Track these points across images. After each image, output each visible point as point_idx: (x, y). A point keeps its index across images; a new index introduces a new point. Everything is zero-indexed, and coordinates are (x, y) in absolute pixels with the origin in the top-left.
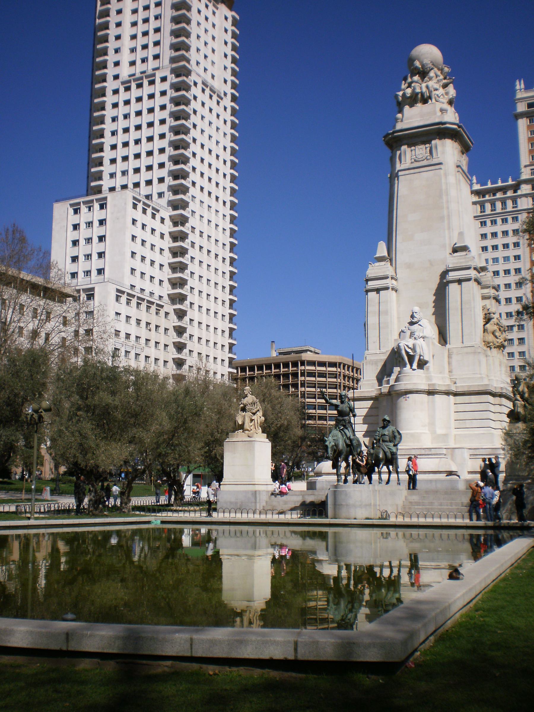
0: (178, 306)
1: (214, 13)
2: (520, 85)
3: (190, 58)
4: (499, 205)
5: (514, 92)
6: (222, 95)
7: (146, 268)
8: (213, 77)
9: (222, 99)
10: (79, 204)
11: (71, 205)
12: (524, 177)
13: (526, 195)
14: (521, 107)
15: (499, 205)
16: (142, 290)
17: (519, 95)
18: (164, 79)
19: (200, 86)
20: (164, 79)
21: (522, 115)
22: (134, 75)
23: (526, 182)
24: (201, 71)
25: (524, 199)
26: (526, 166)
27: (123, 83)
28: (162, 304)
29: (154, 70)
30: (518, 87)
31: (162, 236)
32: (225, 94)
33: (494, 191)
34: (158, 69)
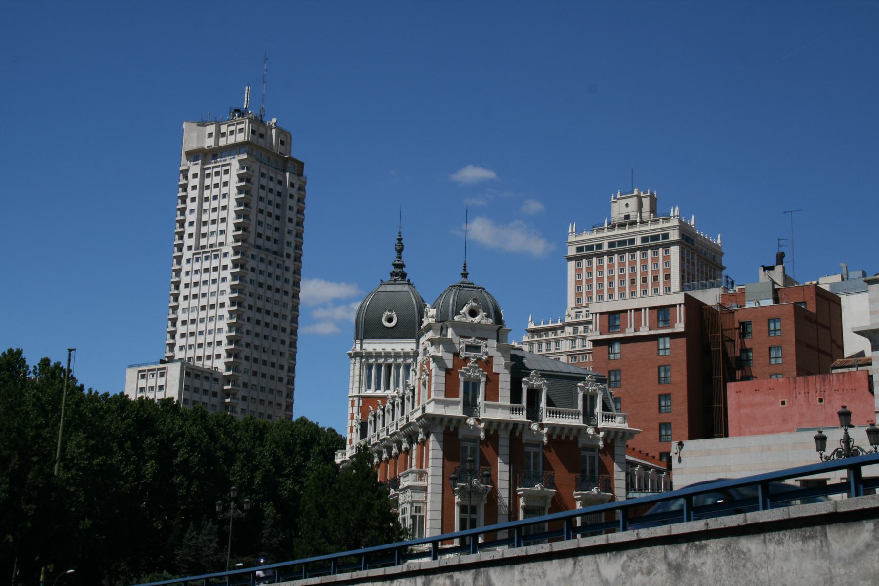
2: (572, 229)
4: (544, 345)
5: (567, 234)
10: (145, 371)
11: (139, 371)
12: (568, 320)
13: (566, 338)
14: (572, 251)
15: (544, 345)
17: (571, 238)
21: (570, 259)
23: (569, 325)
25: (564, 342)
26: (572, 308)
27: (194, 254)
30: (570, 231)
33: (546, 330)
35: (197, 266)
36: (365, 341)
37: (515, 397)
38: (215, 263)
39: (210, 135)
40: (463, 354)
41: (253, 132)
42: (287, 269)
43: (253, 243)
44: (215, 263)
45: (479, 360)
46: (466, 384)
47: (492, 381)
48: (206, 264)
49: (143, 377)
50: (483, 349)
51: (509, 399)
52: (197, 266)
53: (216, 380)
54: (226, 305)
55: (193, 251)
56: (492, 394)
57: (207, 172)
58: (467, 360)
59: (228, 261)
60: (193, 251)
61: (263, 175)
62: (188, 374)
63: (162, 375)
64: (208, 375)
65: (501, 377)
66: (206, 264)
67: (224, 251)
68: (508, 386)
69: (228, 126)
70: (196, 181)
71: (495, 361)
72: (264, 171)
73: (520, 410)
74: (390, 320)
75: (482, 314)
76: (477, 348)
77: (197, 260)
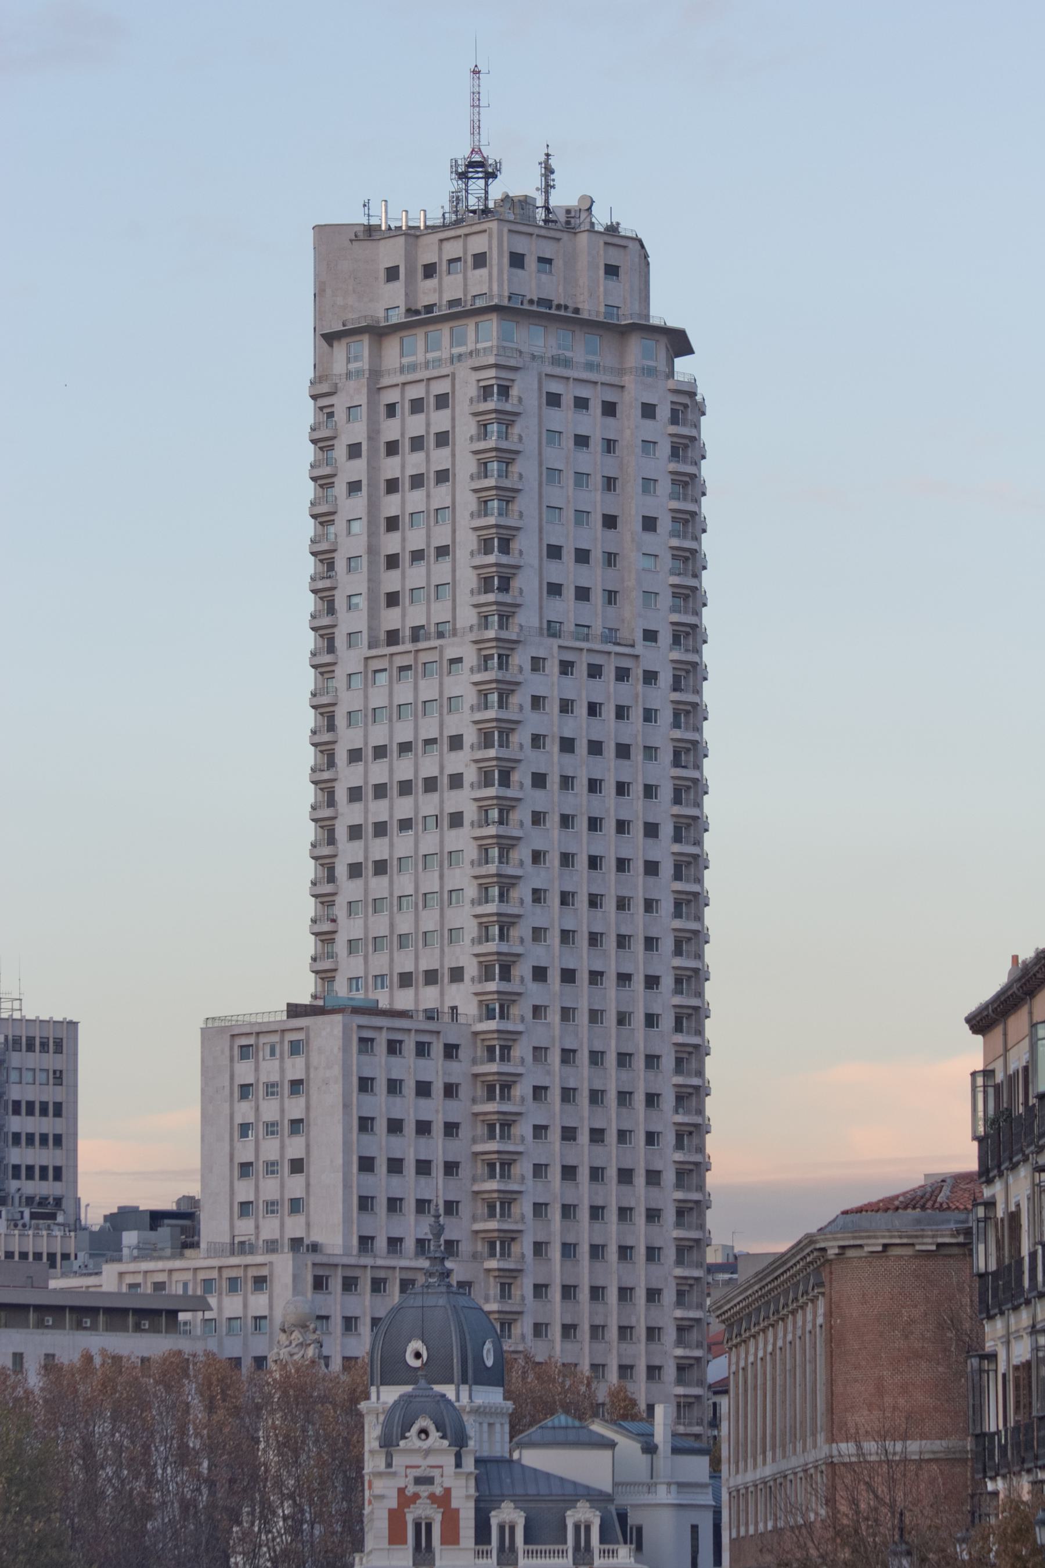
36: (382, 1388)
37: (482, 1534)
39: (392, 274)
40: (411, 1489)
41: (517, 260)
42: (650, 677)
43: (535, 622)
45: (432, 1497)
46: (418, 1526)
47: (451, 1519)
49: (245, 1052)
50: (437, 1480)
51: (473, 1541)
53: (451, 1051)
54: (467, 820)
56: (451, 1537)
58: (416, 1496)
61: (554, 400)
62: (366, 1044)
63: (296, 1048)
65: (462, 1514)
67: (451, 653)
68: (472, 1523)
71: (454, 1493)
72: (555, 387)
73: (488, 1554)
74: (418, 1355)
75: (434, 1434)
76: (429, 1481)
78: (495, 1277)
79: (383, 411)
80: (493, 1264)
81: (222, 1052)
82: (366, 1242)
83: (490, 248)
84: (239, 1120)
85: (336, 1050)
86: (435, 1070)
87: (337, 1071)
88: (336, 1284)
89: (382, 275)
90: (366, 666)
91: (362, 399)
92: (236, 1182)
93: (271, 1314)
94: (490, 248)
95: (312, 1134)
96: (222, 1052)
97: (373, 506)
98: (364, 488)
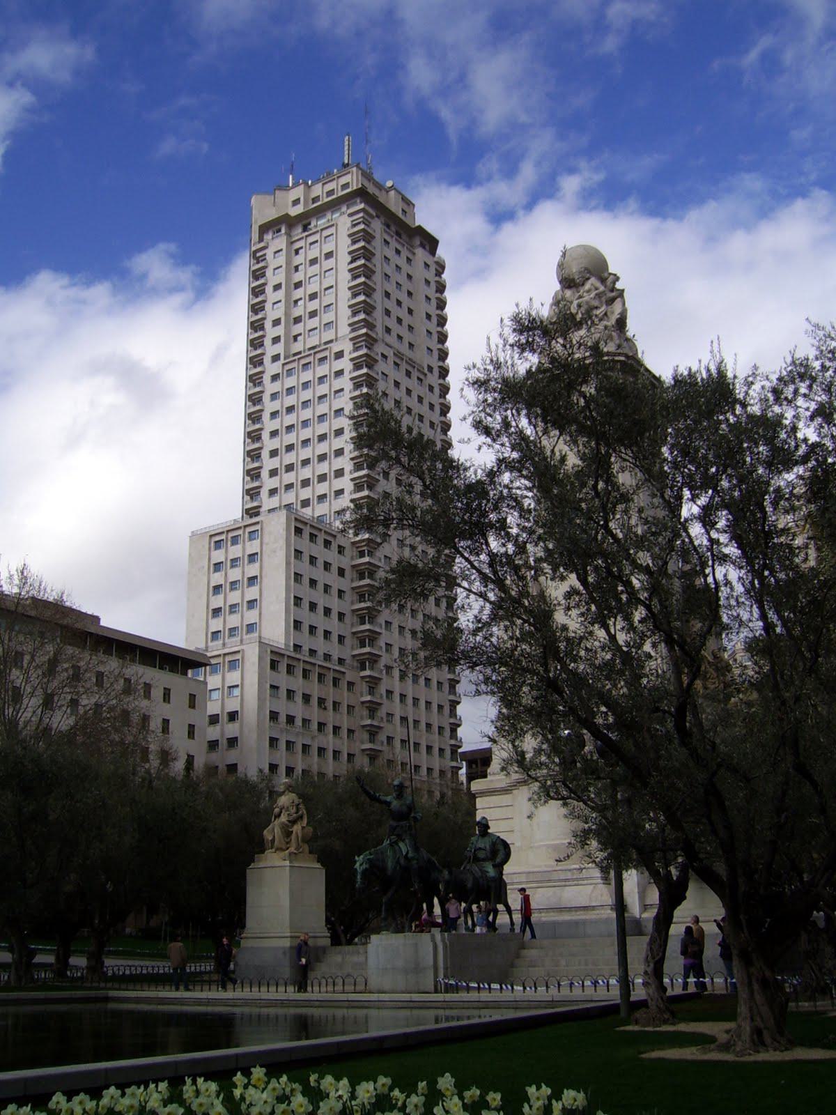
0: (367, 673)
1: (409, 260)
3: (374, 323)
6: (426, 370)
7: (318, 619)
8: (411, 345)
9: (426, 375)
16: (312, 652)
18: (339, 355)
19: (391, 359)
20: (339, 355)
22: (300, 353)
24: (392, 340)
27: (284, 365)
28: (343, 670)
29: (326, 343)
31: (341, 572)
32: (430, 369)
34: (331, 341)
35: (290, 382)
38: (322, 370)
44: (322, 370)
48: (307, 376)
49: (218, 545)
52: (290, 382)
55: (282, 361)
57: (297, 245)
59: (345, 364)
60: (282, 361)
62: (298, 531)
64: (329, 538)
66: (307, 376)
69: (323, 184)
70: (281, 260)
77: (290, 373)
78: (367, 682)
79: (293, 253)
80: (364, 673)
81: (203, 546)
82: (297, 647)
83: (352, 179)
84: (213, 584)
85: (281, 531)
86: (332, 556)
87: (282, 543)
88: (283, 668)
89: (290, 204)
90: (283, 368)
91: (284, 246)
92: (210, 621)
93: (242, 684)
94: (352, 179)
95: (263, 584)
96: (203, 546)
97: (288, 295)
98: (283, 286)
